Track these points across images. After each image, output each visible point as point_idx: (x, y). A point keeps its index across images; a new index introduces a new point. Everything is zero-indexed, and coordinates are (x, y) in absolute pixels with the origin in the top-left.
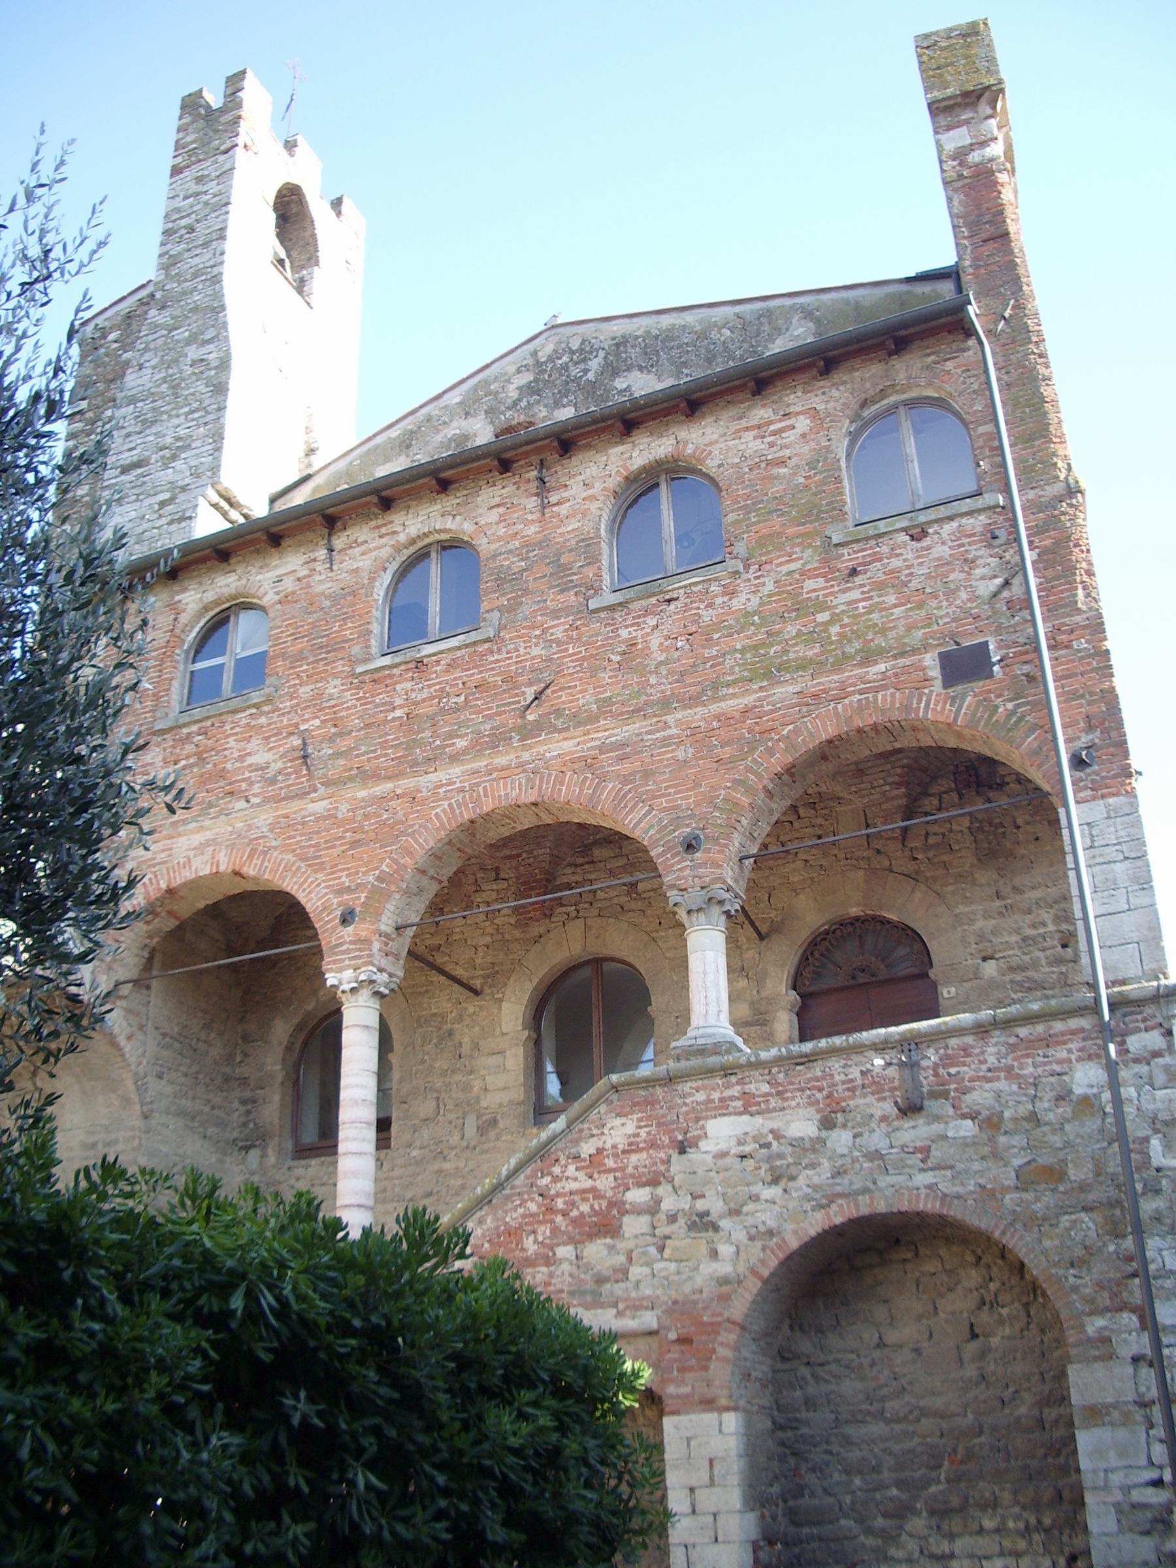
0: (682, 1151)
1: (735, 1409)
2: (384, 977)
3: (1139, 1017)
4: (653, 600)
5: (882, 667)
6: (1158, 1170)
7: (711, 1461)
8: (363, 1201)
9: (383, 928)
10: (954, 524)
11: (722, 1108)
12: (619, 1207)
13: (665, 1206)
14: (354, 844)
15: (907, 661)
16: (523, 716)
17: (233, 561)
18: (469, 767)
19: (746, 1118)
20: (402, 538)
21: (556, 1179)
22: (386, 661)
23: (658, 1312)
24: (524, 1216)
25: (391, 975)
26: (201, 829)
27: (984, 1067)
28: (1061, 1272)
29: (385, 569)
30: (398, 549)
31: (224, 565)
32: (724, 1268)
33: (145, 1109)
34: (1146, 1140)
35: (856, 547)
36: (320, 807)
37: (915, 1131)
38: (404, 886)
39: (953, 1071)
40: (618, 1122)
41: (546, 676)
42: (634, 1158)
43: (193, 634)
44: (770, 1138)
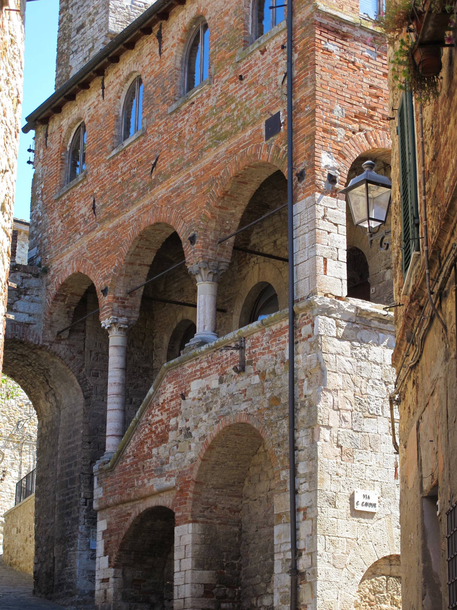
0: (184, 399)
1: (194, 522)
2: (124, 319)
3: (305, 317)
4: (187, 105)
5: (249, 132)
6: (305, 396)
7: (185, 546)
8: (114, 433)
9: (117, 295)
10: (274, 42)
11: (193, 376)
12: (168, 428)
13: (179, 426)
14: (109, 252)
15: (256, 128)
16: (151, 177)
17: (77, 98)
18: (140, 205)
19: (200, 380)
20: (122, 78)
21: (153, 416)
22: (114, 152)
23: (176, 478)
24: (145, 435)
25: (128, 317)
26: (69, 251)
27: (262, 348)
28: (276, 449)
29: (119, 98)
30: (122, 85)
31: (74, 102)
32: (192, 455)
33: (86, 393)
34: (303, 380)
35: (245, 61)
36: (99, 234)
37: (242, 382)
38: (124, 272)
39: (254, 350)
40: (169, 385)
41: (158, 153)
42: (173, 403)
43: (70, 142)
44: (206, 390)
